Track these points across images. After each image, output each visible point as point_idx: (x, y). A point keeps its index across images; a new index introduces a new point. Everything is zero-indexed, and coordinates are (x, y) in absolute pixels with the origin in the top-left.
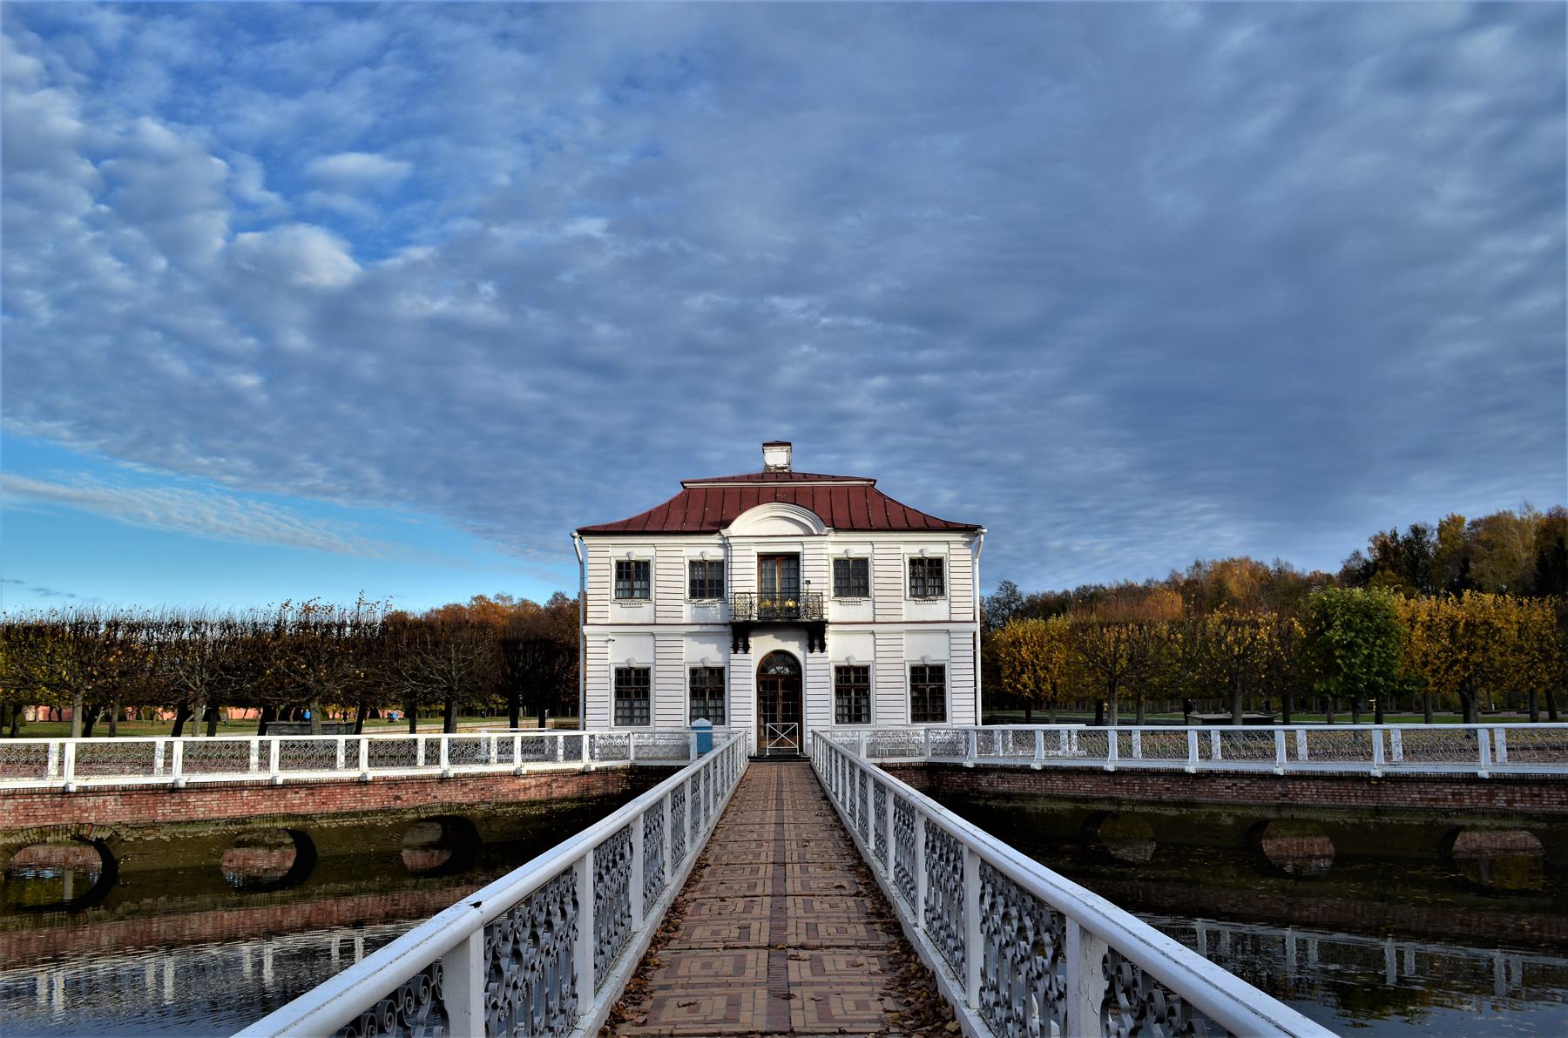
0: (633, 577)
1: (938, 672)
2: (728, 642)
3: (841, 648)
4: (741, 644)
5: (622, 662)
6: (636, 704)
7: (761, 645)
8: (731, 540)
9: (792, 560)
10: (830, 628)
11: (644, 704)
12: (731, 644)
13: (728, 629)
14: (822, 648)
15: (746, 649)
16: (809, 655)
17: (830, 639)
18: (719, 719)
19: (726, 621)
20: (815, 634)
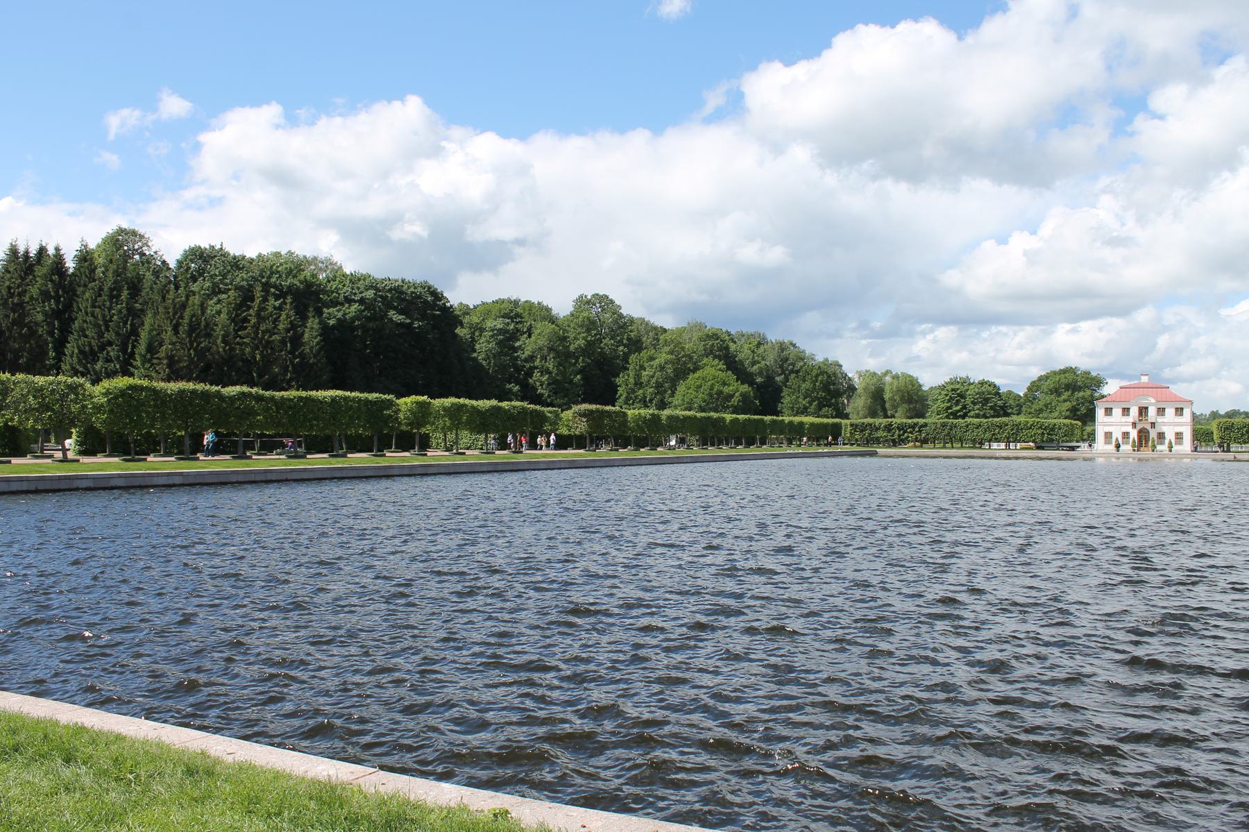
1: (1181, 433)
9: (1146, 408)
20: (1153, 425)
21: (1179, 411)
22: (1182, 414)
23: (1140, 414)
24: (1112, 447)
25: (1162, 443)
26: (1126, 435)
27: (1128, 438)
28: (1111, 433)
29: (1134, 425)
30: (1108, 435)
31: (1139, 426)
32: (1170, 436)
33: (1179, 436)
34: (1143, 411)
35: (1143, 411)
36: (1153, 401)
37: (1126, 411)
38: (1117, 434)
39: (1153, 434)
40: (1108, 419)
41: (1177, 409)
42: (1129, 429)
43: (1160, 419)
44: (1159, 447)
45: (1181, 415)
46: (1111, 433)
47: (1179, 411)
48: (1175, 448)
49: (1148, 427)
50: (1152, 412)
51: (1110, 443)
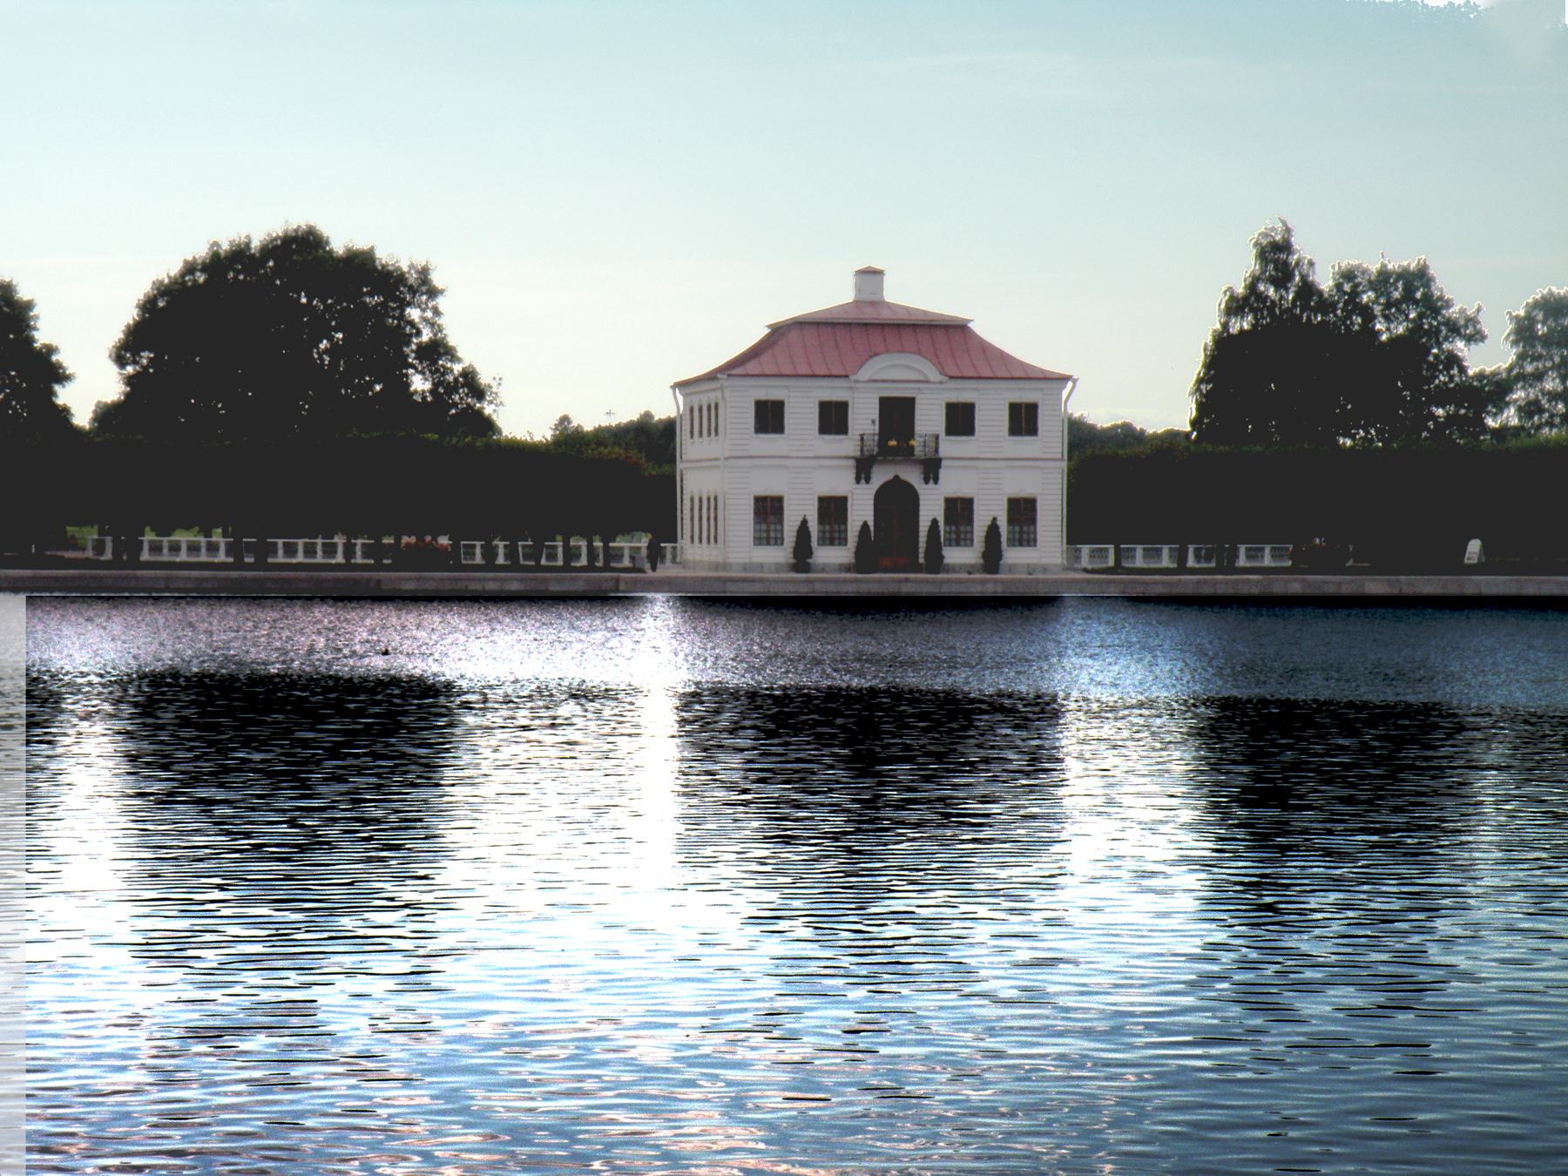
0: (770, 417)
2: (852, 475)
3: (953, 483)
4: (863, 475)
5: (762, 492)
6: (772, 527)
7: (881, 476)
8: (857, 385)
10: (944, 463)
11: (779, 527)
12: (854, 476)
13: (852, 463)
14: (936, 482)
15: (868, 481)
16: (924, 486)
17: (943, 473)
18: (968, 542)
19: (853, 454)
20: (931, 469)
21: (1023, 420)
22: (1032, 430)
23: (884, 434)
24: (779, 555)
25: (963, 540)
26: (833, 509)
27: (843, 519)
28: (778, 501)
29: (863, 469)
30: (768, 509)
31: (881, 476)
32: (990, 510)
33: (1023, 511)
34: (897, 414)
35: (897, 414)
36: (933, 374)
37: (833, 418)
38: (800, 509)
39: (931, 508)
40: (769, 443)
41: (1015, 409)
42: (840, 482)
43: (951, 447)
44: (953, 555)
45: (1032, 430)
46: (778, 501)
47: (1023, 420)
48: (1014, 556)
49: (912, 476)
50: (929, 420)
51: (779, 541)
